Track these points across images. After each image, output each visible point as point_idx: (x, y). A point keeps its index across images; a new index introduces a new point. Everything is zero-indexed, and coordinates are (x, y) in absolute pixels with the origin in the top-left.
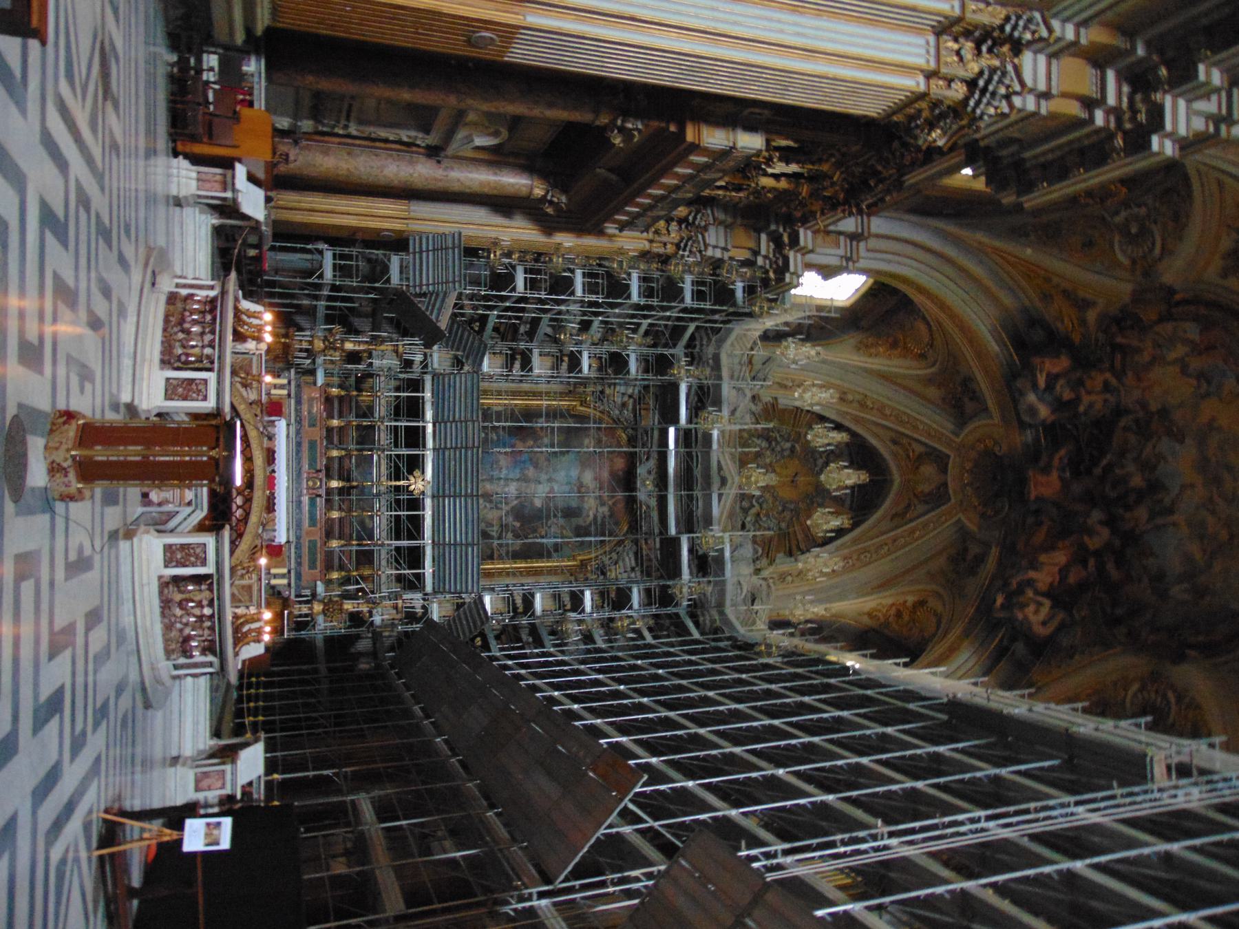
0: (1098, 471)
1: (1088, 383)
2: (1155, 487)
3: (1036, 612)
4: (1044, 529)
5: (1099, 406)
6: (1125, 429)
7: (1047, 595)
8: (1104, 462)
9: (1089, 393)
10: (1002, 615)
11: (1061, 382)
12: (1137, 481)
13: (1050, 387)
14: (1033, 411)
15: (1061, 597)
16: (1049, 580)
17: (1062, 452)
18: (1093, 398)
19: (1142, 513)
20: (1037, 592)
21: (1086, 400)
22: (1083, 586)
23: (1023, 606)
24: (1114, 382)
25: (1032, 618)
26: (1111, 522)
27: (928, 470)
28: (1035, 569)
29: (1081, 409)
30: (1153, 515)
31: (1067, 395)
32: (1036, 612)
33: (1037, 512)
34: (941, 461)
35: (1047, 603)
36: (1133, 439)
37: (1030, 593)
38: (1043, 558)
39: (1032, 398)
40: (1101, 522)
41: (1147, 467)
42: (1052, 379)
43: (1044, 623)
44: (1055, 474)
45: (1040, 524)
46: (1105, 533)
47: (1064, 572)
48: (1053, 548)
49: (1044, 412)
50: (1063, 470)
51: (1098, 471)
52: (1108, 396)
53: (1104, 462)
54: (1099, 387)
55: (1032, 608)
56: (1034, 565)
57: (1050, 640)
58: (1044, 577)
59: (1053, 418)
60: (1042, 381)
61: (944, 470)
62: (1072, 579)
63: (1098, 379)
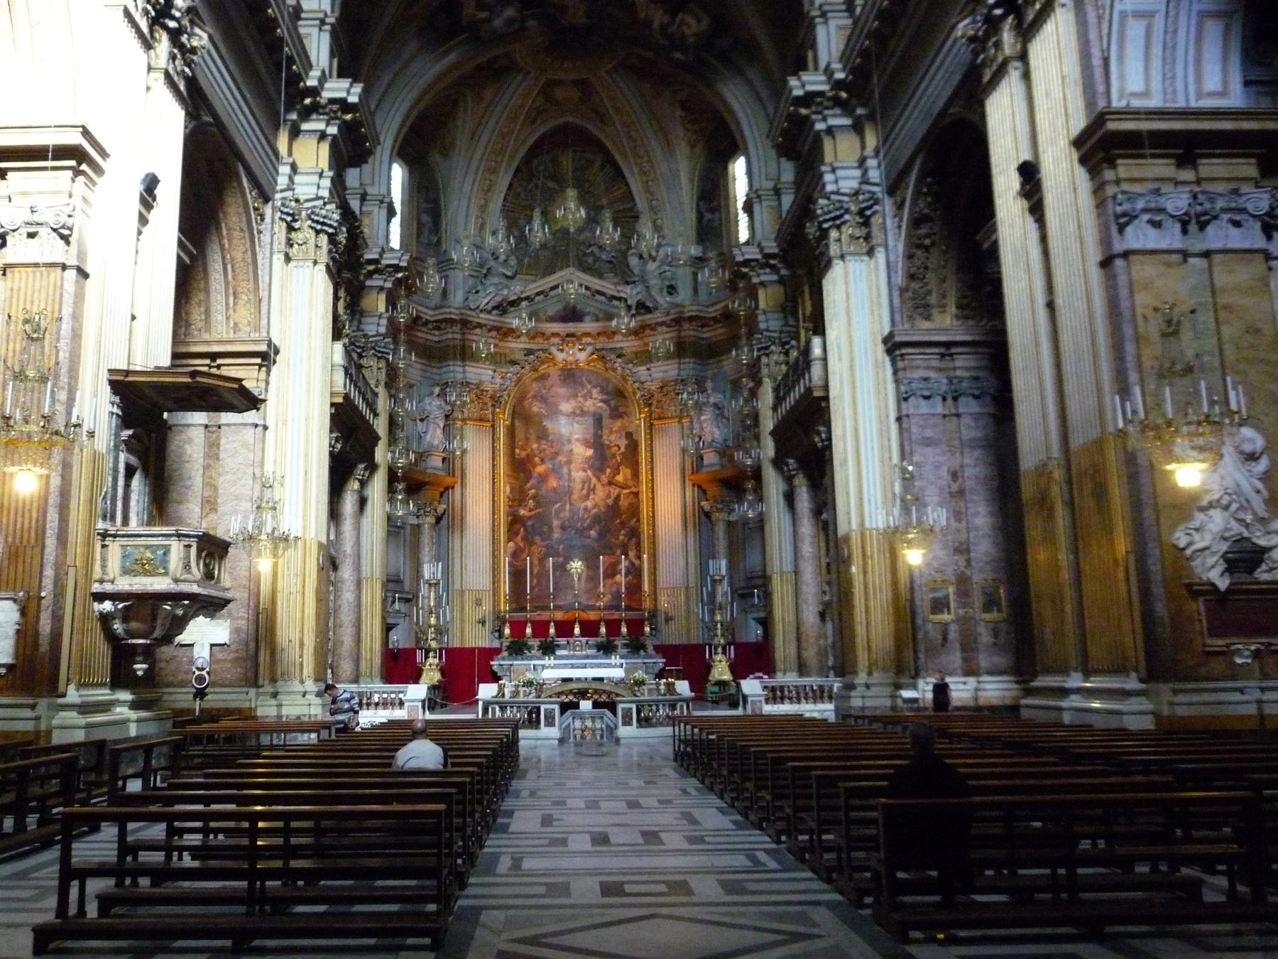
3: (689, 26)
16: (661, 12)
20: (672, 24)
23: (683, 37)
27: (559, 93)
28: (652, 22)
34: (552, 84)
35: (680, 17)
37: (673, 29)
38: (642, 15)
39: (498, 22)
43: (699, 21)
55: (685, 28)
56: (648, 23)
58: (659, 17)
60: (484, 15)
61: (560, 83)
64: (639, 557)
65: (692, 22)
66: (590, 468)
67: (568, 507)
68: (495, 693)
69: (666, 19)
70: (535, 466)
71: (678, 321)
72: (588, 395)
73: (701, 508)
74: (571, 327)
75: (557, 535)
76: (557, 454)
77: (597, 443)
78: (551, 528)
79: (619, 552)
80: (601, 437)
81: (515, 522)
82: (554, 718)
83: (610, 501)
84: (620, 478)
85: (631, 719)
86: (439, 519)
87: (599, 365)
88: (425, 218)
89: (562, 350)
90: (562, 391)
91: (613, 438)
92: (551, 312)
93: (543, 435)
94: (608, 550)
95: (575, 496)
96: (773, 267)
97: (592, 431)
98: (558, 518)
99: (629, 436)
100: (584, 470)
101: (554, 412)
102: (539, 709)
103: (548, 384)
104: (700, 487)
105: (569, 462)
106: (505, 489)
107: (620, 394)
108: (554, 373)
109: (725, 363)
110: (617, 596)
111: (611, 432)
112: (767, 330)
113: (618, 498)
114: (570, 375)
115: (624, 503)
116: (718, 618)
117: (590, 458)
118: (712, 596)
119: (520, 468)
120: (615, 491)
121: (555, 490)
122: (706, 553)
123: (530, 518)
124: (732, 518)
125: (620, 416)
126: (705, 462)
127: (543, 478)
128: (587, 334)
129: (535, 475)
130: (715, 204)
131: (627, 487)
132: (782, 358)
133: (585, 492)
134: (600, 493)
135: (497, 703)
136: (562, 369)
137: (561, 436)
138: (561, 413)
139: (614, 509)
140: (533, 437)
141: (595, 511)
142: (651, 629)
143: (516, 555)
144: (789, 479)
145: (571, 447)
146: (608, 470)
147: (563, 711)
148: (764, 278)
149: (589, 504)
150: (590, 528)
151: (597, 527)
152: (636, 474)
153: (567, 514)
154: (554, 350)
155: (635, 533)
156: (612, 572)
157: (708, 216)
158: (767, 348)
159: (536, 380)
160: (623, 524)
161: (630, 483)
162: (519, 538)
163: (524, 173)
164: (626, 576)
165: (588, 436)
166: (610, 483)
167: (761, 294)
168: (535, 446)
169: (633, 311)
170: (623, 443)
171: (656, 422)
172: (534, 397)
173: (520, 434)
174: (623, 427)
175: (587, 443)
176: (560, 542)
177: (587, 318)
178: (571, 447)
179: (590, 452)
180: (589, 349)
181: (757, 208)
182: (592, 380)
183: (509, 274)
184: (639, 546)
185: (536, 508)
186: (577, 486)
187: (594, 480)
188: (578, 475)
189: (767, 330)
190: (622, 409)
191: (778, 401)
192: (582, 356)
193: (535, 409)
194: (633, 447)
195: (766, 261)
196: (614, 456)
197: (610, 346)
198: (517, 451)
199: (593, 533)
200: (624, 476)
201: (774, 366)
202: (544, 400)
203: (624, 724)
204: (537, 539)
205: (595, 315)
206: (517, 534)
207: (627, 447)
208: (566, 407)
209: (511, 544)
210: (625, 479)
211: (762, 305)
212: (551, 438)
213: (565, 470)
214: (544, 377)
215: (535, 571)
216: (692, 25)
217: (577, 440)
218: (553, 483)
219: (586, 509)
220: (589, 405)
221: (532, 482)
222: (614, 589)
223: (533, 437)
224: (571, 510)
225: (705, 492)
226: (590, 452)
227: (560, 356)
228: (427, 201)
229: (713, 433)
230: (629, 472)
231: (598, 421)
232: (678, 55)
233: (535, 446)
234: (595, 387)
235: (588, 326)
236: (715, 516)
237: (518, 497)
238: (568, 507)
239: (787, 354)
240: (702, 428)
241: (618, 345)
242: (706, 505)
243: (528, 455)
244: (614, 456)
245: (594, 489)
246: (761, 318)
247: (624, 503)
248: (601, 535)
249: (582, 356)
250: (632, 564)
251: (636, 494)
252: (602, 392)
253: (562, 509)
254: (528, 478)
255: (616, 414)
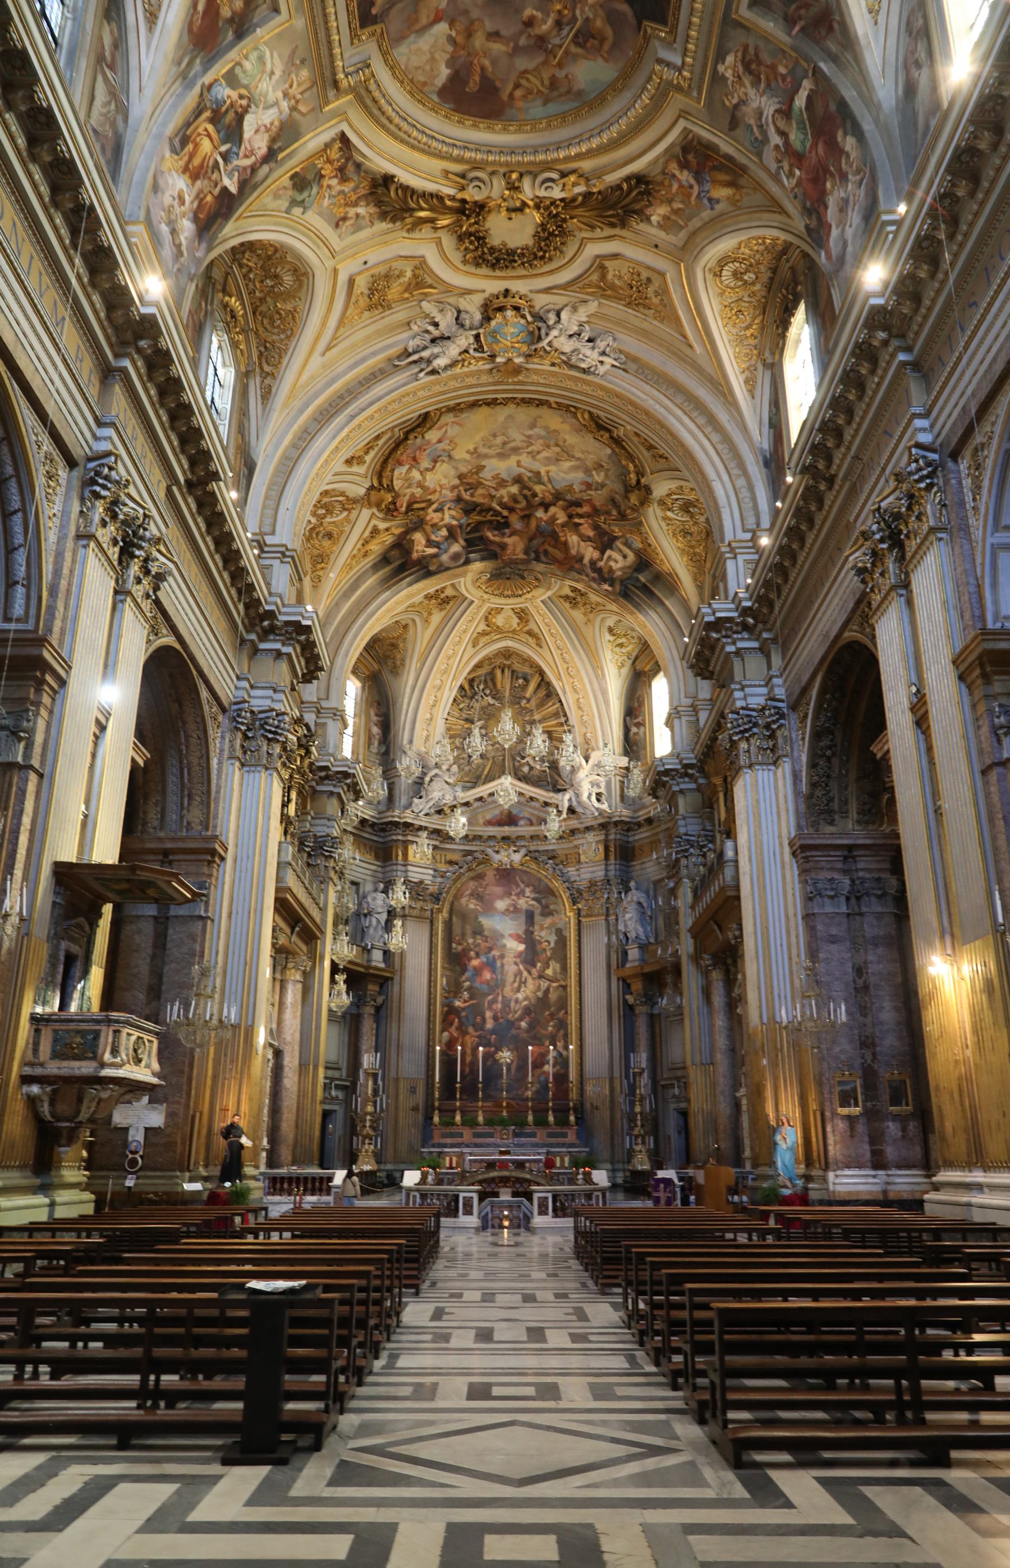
0: (505, 513)
1: (436, 521)
2: (518, 480)
3: (616, 562)
4: (550, 549)
5: (453, 513)
6: (472, 495)
7: (603, 553)
8: (498, 508)
9: (442, 519)
10: (618, 587)
11: (433, 537)
12: (514, 489)
13: (437, 545)
14: (456, 557)
15: (605, 542)
16: (591, 549)
17: (489, 535)
18: (447, 517)
19: (538, 488)
20: (601, 559)
21: (447, 519)
22: (596, 527)
23: (611, 570)
24: (434, 506)
25: (620, 565)
26: (546, 506)
29: (455, 523)
30: (540, 482)
31: (444, 532)
32: (616, 562)
33: (536, 552)
35: (608, 552)
36: (480, 491)
37: (601, 564)
38: (573, 552)
39: (445, 558)
40: (546, 511)
41: (502, 483)
42: (430, 543)
43: (625, 557)
44: (507, 540)
45: (546, 552)
46: (553, 510)
47: (585, 539)
48: (565, 544)
49: (456, 548)
50: (503, 535)
51: (505, 513)
52: (446, 508)
53: (498, 508)
54: (439, 515)
55: (612, 564)
56: (580, 559)
57: (638, 553)
58: (589, 553)
59: (462, 542)
62: (591, 533)
63: (432, 516)
64: (566, 1048)
65: (619, 558)
66: (523, 962)
67: (500, 998)
68: (417, 1180)
69: (596, 555)
70: (470, 959)
71: (603, 826)
72: (522, 893)
73: (625, 1001)
74: (507, 830)
75: (490, 1025)
76: (490, 949)
77: (529, 939)
78: (484, 1020)
79: (547, 1043)
80: (532, 933)
81: (450, 1012)
82: (472, 1206)
83: (540, 994)
84: (549, 972)
85: (547, 1208)
86: (378, 1009)
87: (534, 866)
88: (375, 730)
89: (497, 852)
90: (498, 890)
91: (543, 933)
92: (488, 817)
93: (478, 931)
94: (536, 1040)
95: (508, 990)
96: (690, 776)
97: (524, 928)
98: (490, 1008)
99: (559, 932)
100: (516, 964)
101: (489, 909)
102: (457, 1197)
103: (484, 883)
104: (624, 981)
105: (502, 956)
106: (441, 982)
107: (551, 892)
108: (490, 875)
109: (648, 865)
110: (545, 1087)
111: (542, 928)
112: (686, 834)
113: (547, 991)
114: (506, 875)
115: (553, 996)
116: (638, 1109)
117: (520, 954)
118: (633, 1088)
119: (457, 961)
120: (544, 984)
121: (488, 982)
122: (629, 1046)
123: (463, 1009)
124: (655, 1011)
125: (550, 913)
126: (630, 958)
127: (478, 971)
128: (520, 838)
129: (470, 968)
130: (640, 719)
131: (556, 980)
132: (700, 860)
133: (516, 985)
134: (531, 985)
135: (418, 1190)
136: (497, 869)
137: (495, 931)
138: (496, 909)
139: (543, 1001)
140: (469, 932)
141: (525, 1003)
142: (577, 1118)
143: (450, 1044)
144: (706, 973)
145: (505, 941)
146: (539, 965)
147: (481, 1200)
148: (683, 786)
149: (520, 996)
150: (521, 1019)
151: (527, 1019)
152: (564, 968)
153: (499, 1006)
154: (490, 851)
155: (563, 1025)
156: (540, 1062)
157: (634, 730)
158: (686, 850)
159: (473, 879)
160: (552, 1015)
161: (559, 977)
162: (453, 1029)
163: (468, 691)
164: (554, 1066)
165: (521, 932)
166: (541, 977)
167: (681, 801)
168: (471, 941)
169: (564, 815)
170: (553, 939)
171: (583, 920)
172: (472, 895)
173: (457, 930)
174: (553, 924)
175: (518, 938)
176: (493, 1031)
177: (522, 822)
178: (505, 941)
179: (522, 947)
180: (523, 851)
181: (676, 722)
182: (525, 879)
183: (451, 781)
184: (566, 1036)
185: (471, 998)
186: (510, 978)
187: (525, 974)
188: (511, 968)
189: (686, 834)
190: (552, 907)
191: (697, 897)
192: (517, 858)
193: (472, 906)
194: (562, 941)
195: (685, 771)
196: (545, 950)
197: (541, 848)
198: (454, 945)
199: (523, 1024)
200: (554, 969)
201: (692, 865)
202: (479, 897)
203: (540, 1214)
204: (471, 1030)
205: (530, 820)
206: (451, 1024)
207: (556, 942)
208: (501, 905)
209: (446, 1034)
210: (555, 972)
211: (682, 810)
212: (486, 933)
213: (499, 964)
214: (480, 877)
215: (468, 1059)
216: (618, 561)
217: (511, 935)
218: (487, 975)
219: (517, 1001)
220: (522, 903)
221: (468, 974)
222: (542, 1078)
223: (469, 932)
224: (503, 1002)
225: (629, 986)
226: (522, 947)
227: (497, 857)
228: (377, 715)
229: (636, 930)
230: (558, 967)
231: (530, 916)
232: (606, 587)
233: (471, 941)
234: (527, 886)
235: (523, 829)
236: (638, 1010)
237: (454, 989)
238: (500, 998)
239: (704, 856)
240: (626, 926)
241: (550, 847)
242: (631, 999)
243: (464, 950)
244: (545, 950)
245: (525, 983)
246: (681, 823)
247: (553, 996)
248: (532, 1026)
249: (517, 858)
250: (561, 1055)
251: (565, 987)
252: (533, 891)
253: (494, 1001)
254: (464, 969)
255: (547, 912)
